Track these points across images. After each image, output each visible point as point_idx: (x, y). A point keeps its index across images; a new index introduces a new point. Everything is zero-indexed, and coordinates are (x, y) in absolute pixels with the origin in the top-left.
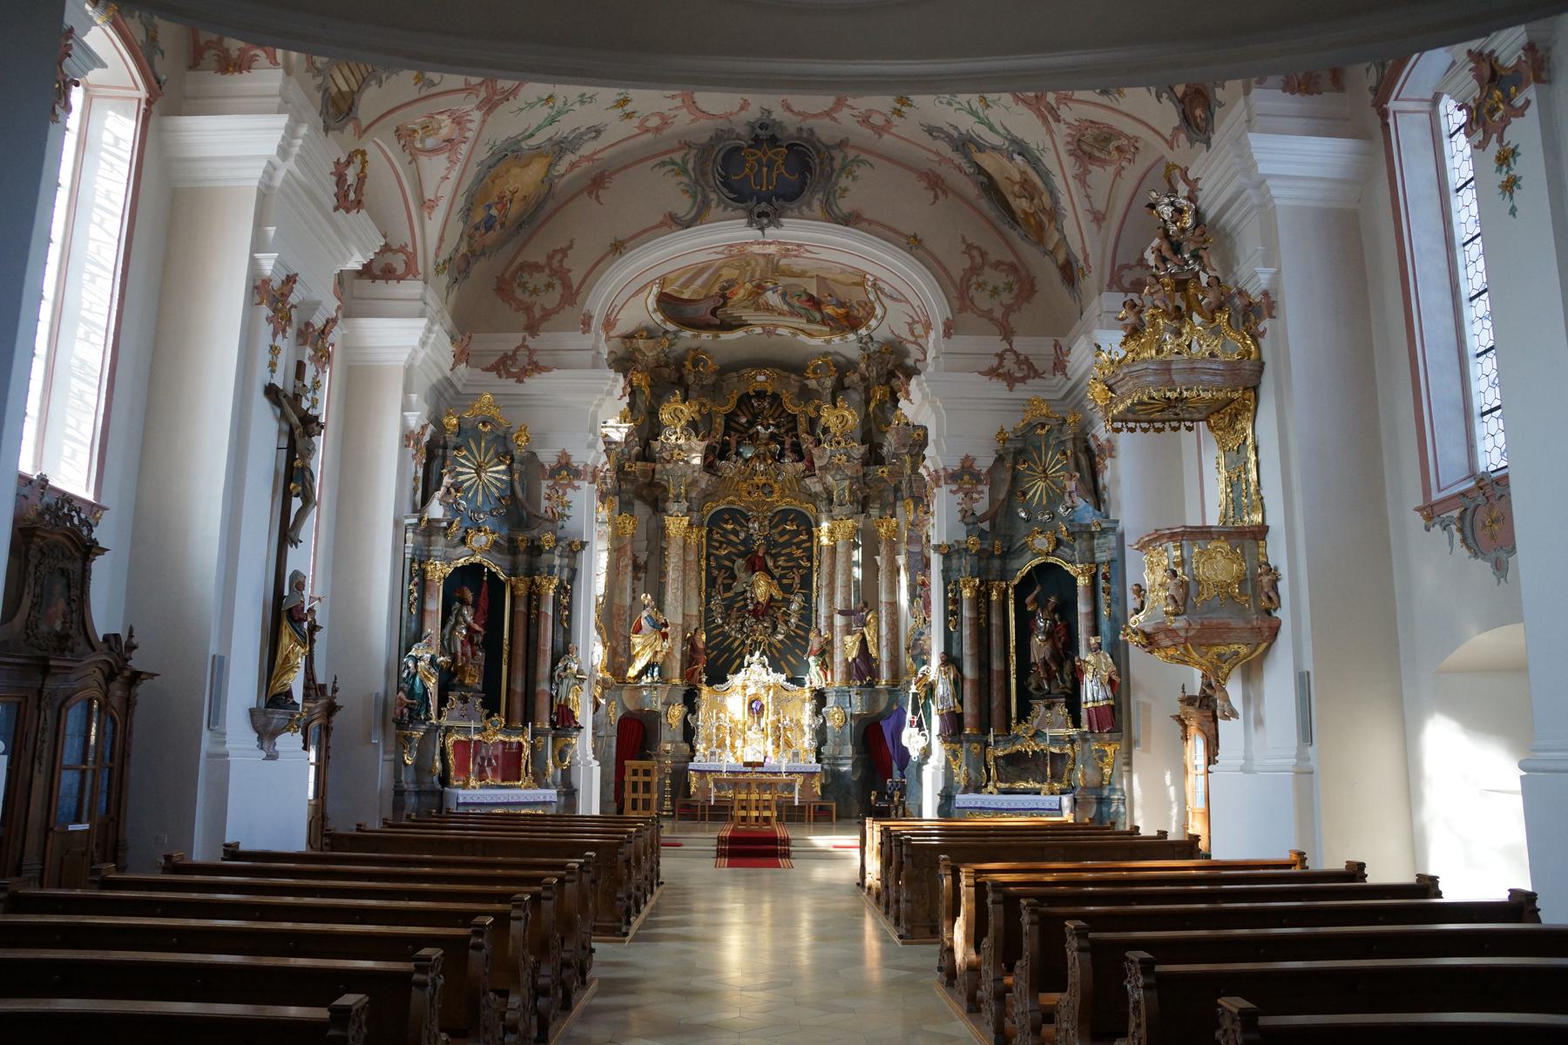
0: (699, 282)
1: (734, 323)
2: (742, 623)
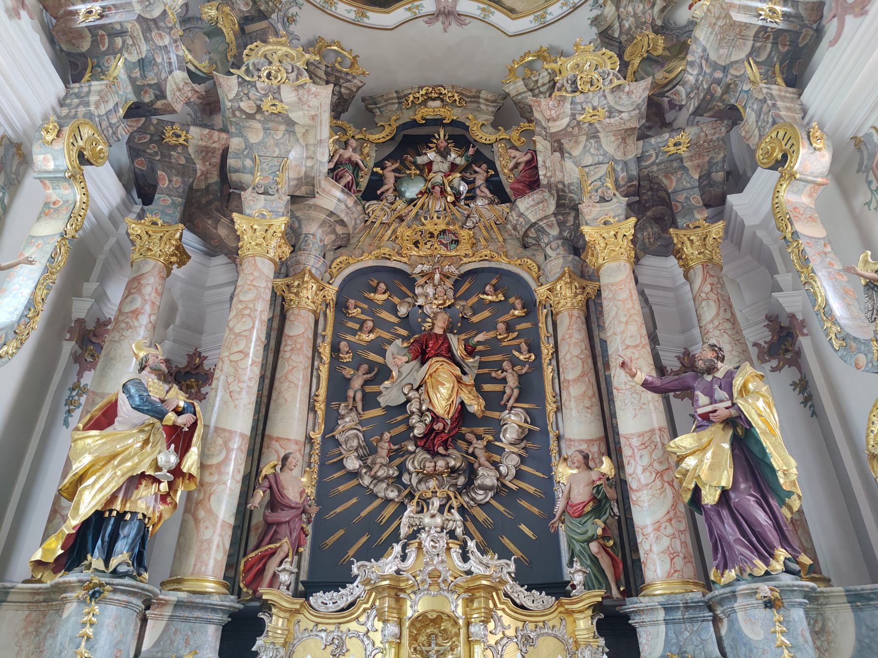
2: (402, 468)
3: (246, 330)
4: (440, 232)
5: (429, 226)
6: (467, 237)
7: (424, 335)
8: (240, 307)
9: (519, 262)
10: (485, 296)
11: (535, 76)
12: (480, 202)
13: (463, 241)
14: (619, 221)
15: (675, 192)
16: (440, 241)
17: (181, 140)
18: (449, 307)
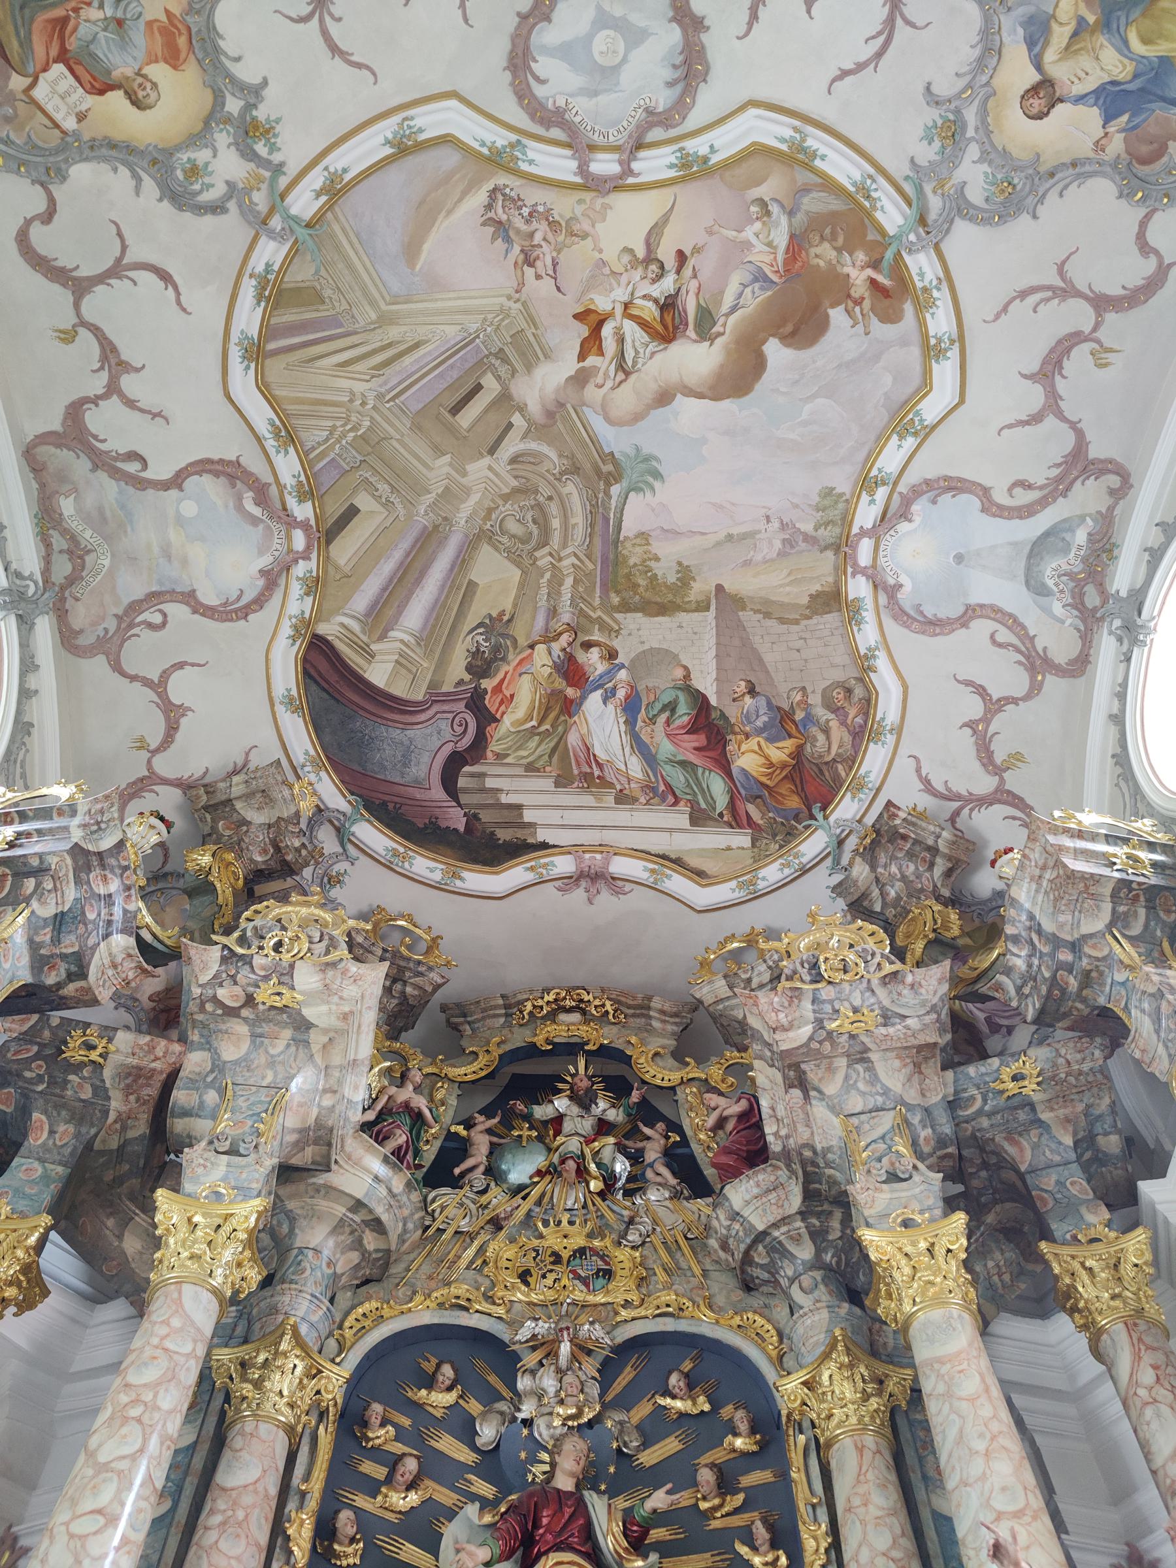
0: (414, 616)
1: (503, 835)
3: (124, 1457)
4: (575, 1252)
5: (552, 1240)
6: (628, 1265)
7: (531, 1495)
8: (124, 1399)
9: (737, 1320)
10: (668, 1401)
11: (745, 972)
12: (653, 1195)
13: (620, 1273)
14: (932, 1220)
15: (1033, 1171)
16: (573, 1272)
17: (94, 1056)
18: (590, 1424)
